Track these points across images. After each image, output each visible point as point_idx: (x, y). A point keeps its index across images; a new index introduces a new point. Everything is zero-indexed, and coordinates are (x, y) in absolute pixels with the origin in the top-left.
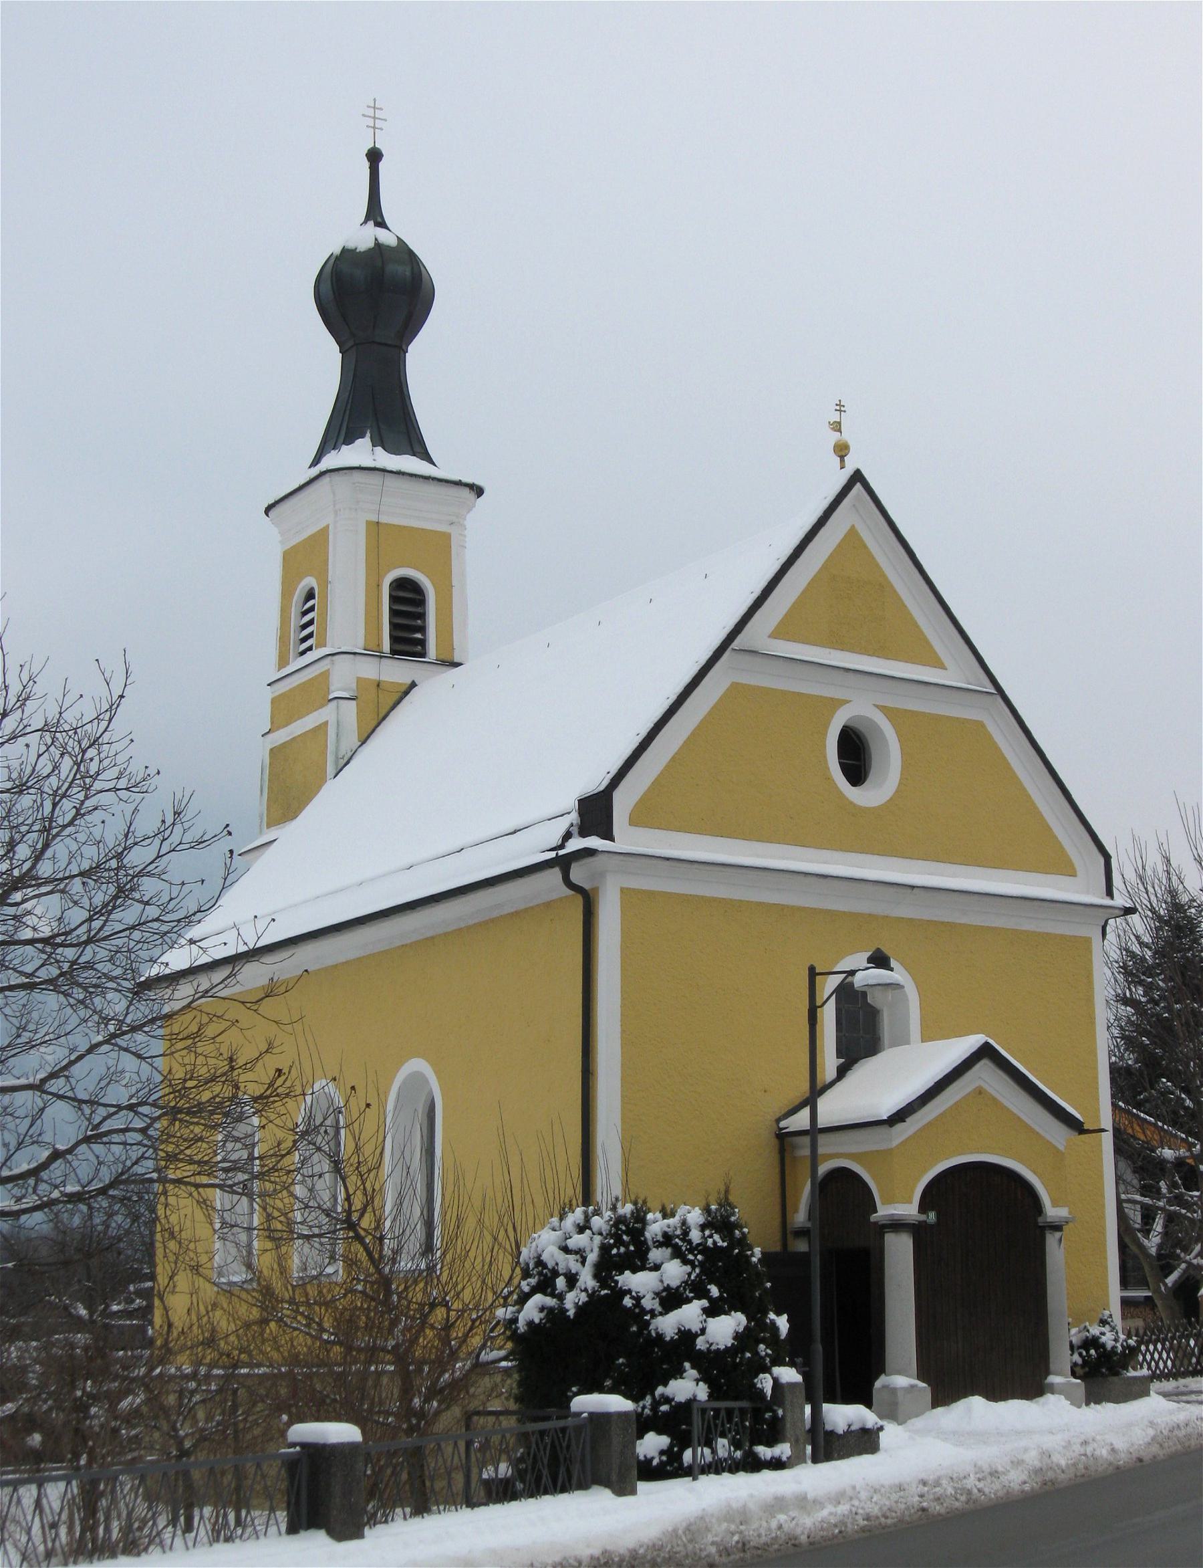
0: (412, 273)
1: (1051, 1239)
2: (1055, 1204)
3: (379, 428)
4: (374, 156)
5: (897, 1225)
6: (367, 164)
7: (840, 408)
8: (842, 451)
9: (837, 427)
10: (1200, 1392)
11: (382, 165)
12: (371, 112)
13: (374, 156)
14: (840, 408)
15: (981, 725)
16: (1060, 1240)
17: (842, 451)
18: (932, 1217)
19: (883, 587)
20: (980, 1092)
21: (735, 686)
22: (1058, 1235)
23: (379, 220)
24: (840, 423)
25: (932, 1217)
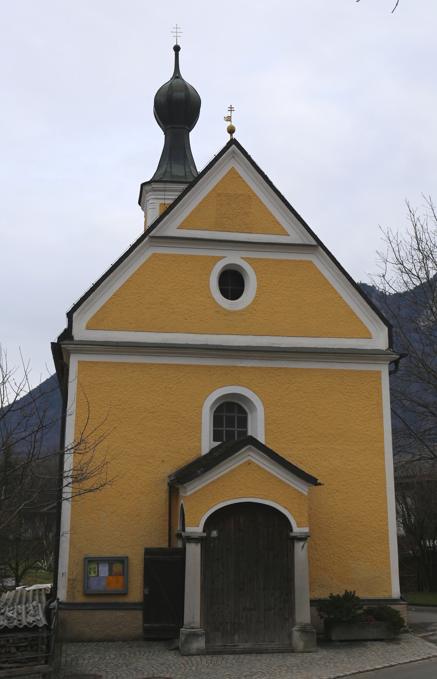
0: (186, 95)
1: (298, 546)
2: (299, 526)
3: (171, 163)
4: (177, 49)
5: (190, 539)
6: (174, 52)
7: (231, 109)
8: (231, 131)
9: (229, 119)
10: (434, 630)
11: (180, 52)
12: (175, 30)
13: (177, 49)
14: (231, 109)
15: (311, 262)
16: (303, 547)
17: (231, 131)
18: (214, 533)
19: (251, 197)
20: (249, 463)
21: (154, 255)
22: (301, 544)
23: (177, 75)
24: (230, 117)
25: (214, 533)
